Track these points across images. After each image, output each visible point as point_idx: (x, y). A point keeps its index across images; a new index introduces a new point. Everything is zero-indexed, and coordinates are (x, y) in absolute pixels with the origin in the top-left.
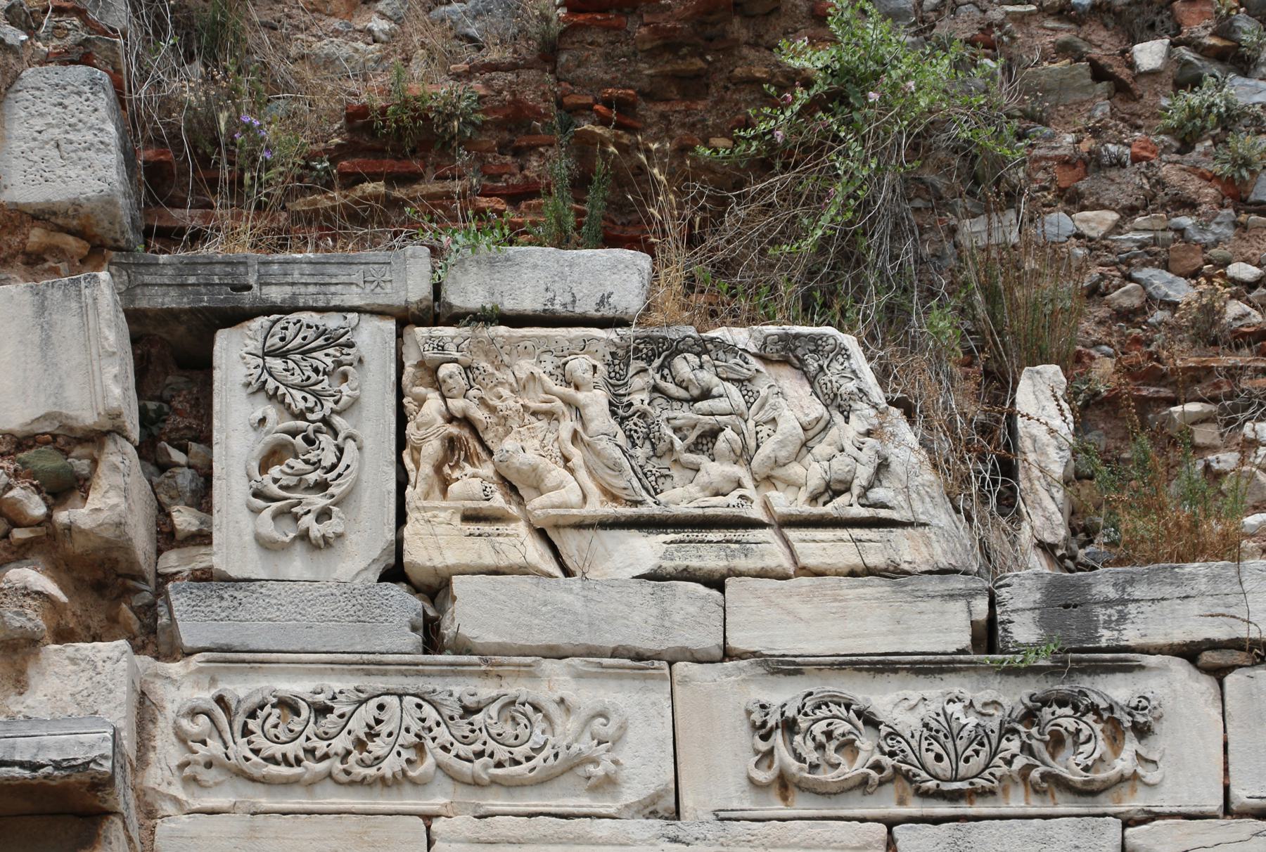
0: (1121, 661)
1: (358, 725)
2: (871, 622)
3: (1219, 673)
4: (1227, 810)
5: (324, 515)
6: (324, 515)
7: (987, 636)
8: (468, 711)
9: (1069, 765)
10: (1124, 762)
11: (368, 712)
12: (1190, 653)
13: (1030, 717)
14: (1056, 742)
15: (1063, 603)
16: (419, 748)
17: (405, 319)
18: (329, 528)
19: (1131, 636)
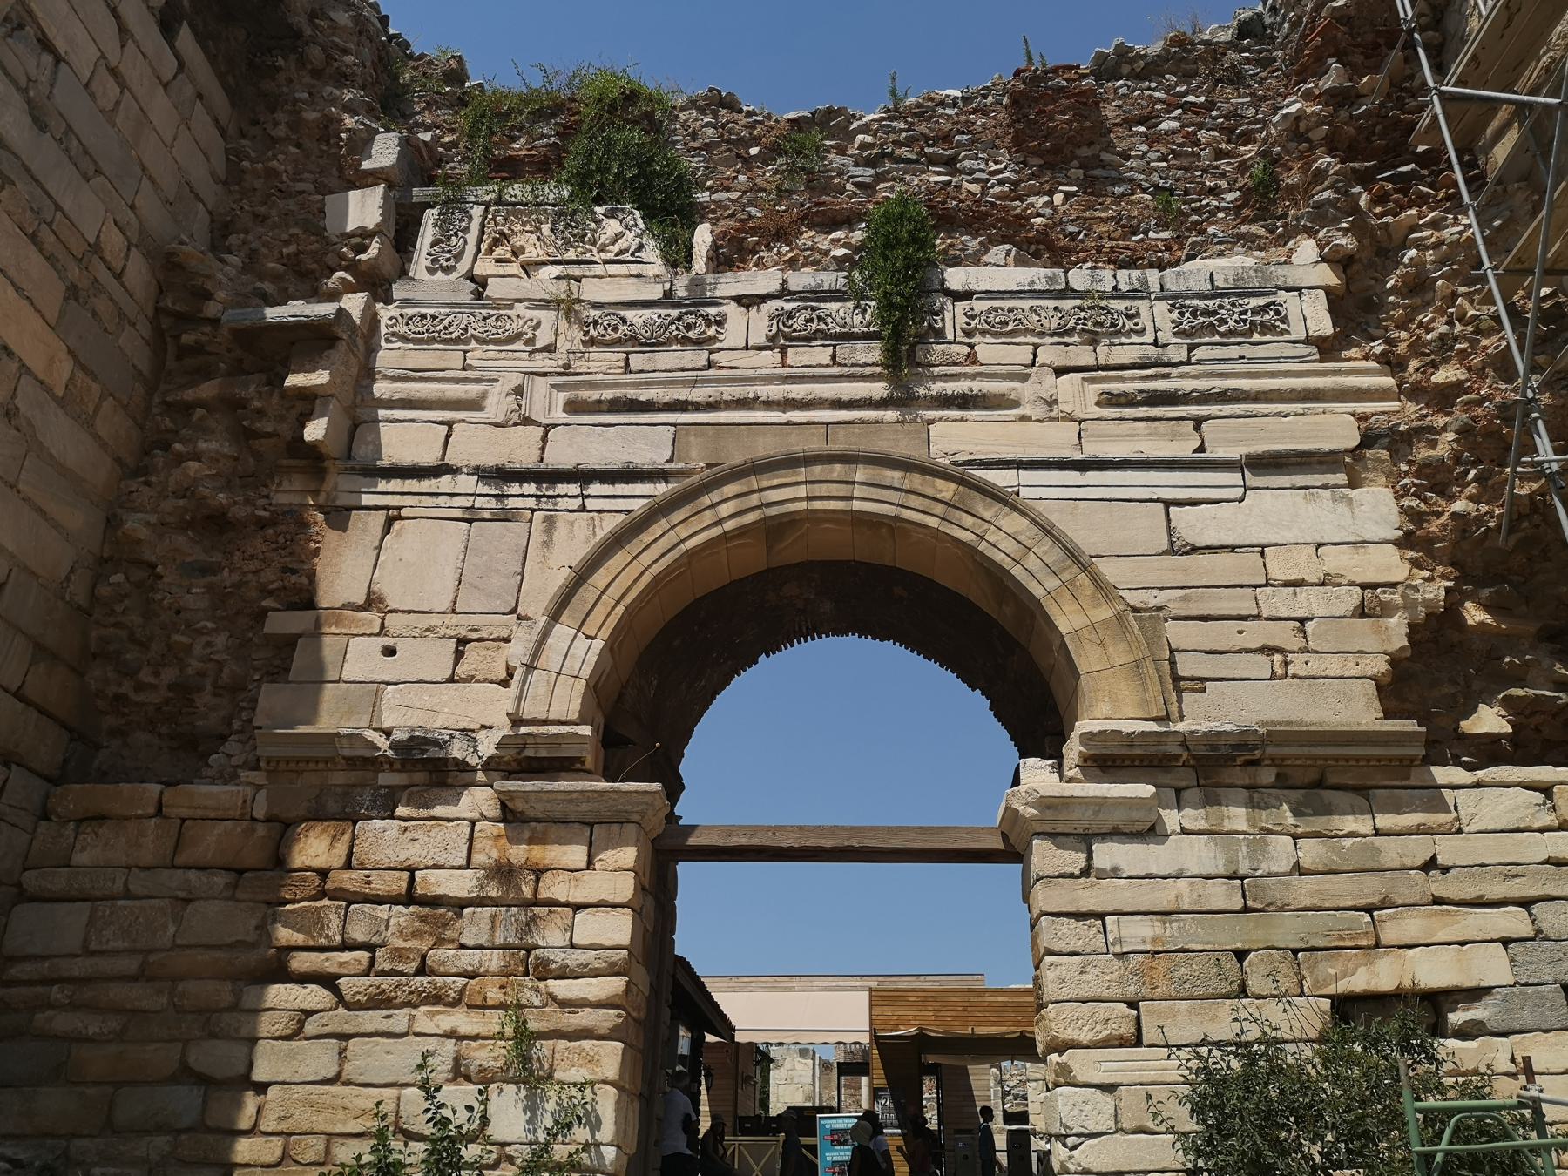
0: (714, 302)
1: (446, 323)
2: (631, 291)
3: (747, 307)
4: (747, 348)
5: (448, 260)
6: (448, 260)
7: (668, 294)
8: (485, 318)
9: (691, 334)
10: (711, 331)
11: (450, 319)
12: (739, 300)
13: (679, 319)
14: (689, 327)
15: (697, 283)
16: (466, 330)
17: (487, 205)
18: (452, 262)
19: (717, 294)
